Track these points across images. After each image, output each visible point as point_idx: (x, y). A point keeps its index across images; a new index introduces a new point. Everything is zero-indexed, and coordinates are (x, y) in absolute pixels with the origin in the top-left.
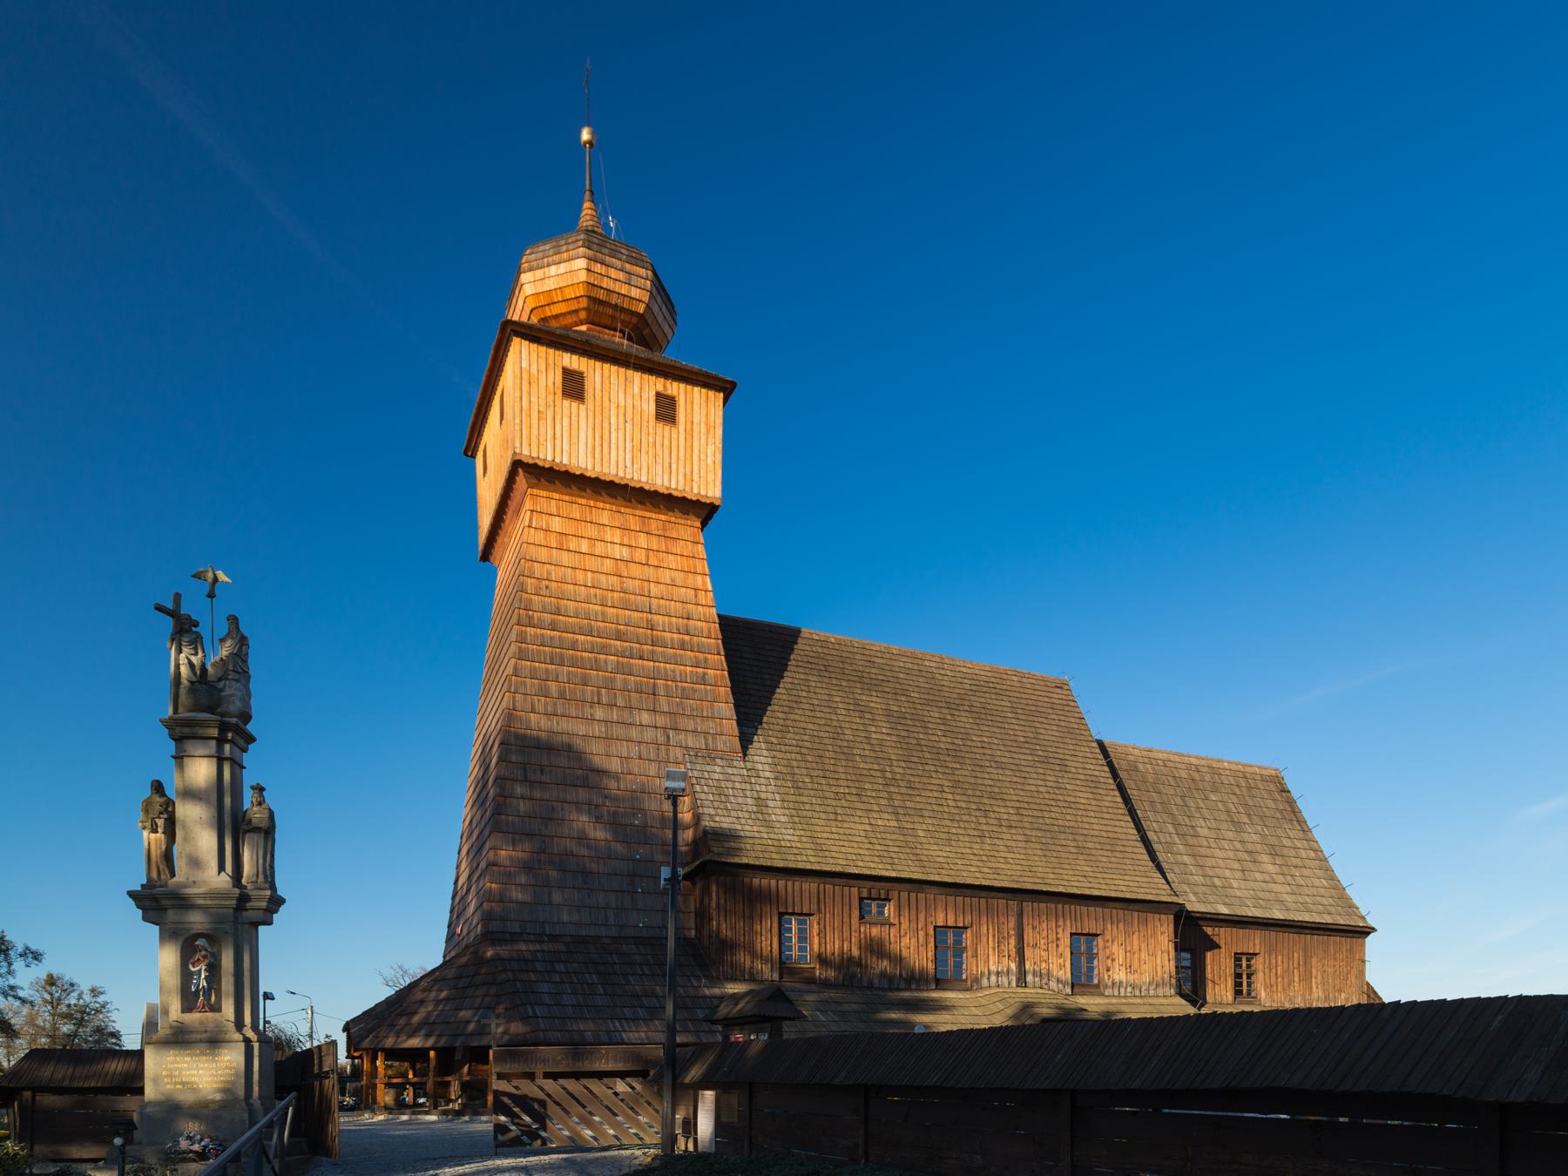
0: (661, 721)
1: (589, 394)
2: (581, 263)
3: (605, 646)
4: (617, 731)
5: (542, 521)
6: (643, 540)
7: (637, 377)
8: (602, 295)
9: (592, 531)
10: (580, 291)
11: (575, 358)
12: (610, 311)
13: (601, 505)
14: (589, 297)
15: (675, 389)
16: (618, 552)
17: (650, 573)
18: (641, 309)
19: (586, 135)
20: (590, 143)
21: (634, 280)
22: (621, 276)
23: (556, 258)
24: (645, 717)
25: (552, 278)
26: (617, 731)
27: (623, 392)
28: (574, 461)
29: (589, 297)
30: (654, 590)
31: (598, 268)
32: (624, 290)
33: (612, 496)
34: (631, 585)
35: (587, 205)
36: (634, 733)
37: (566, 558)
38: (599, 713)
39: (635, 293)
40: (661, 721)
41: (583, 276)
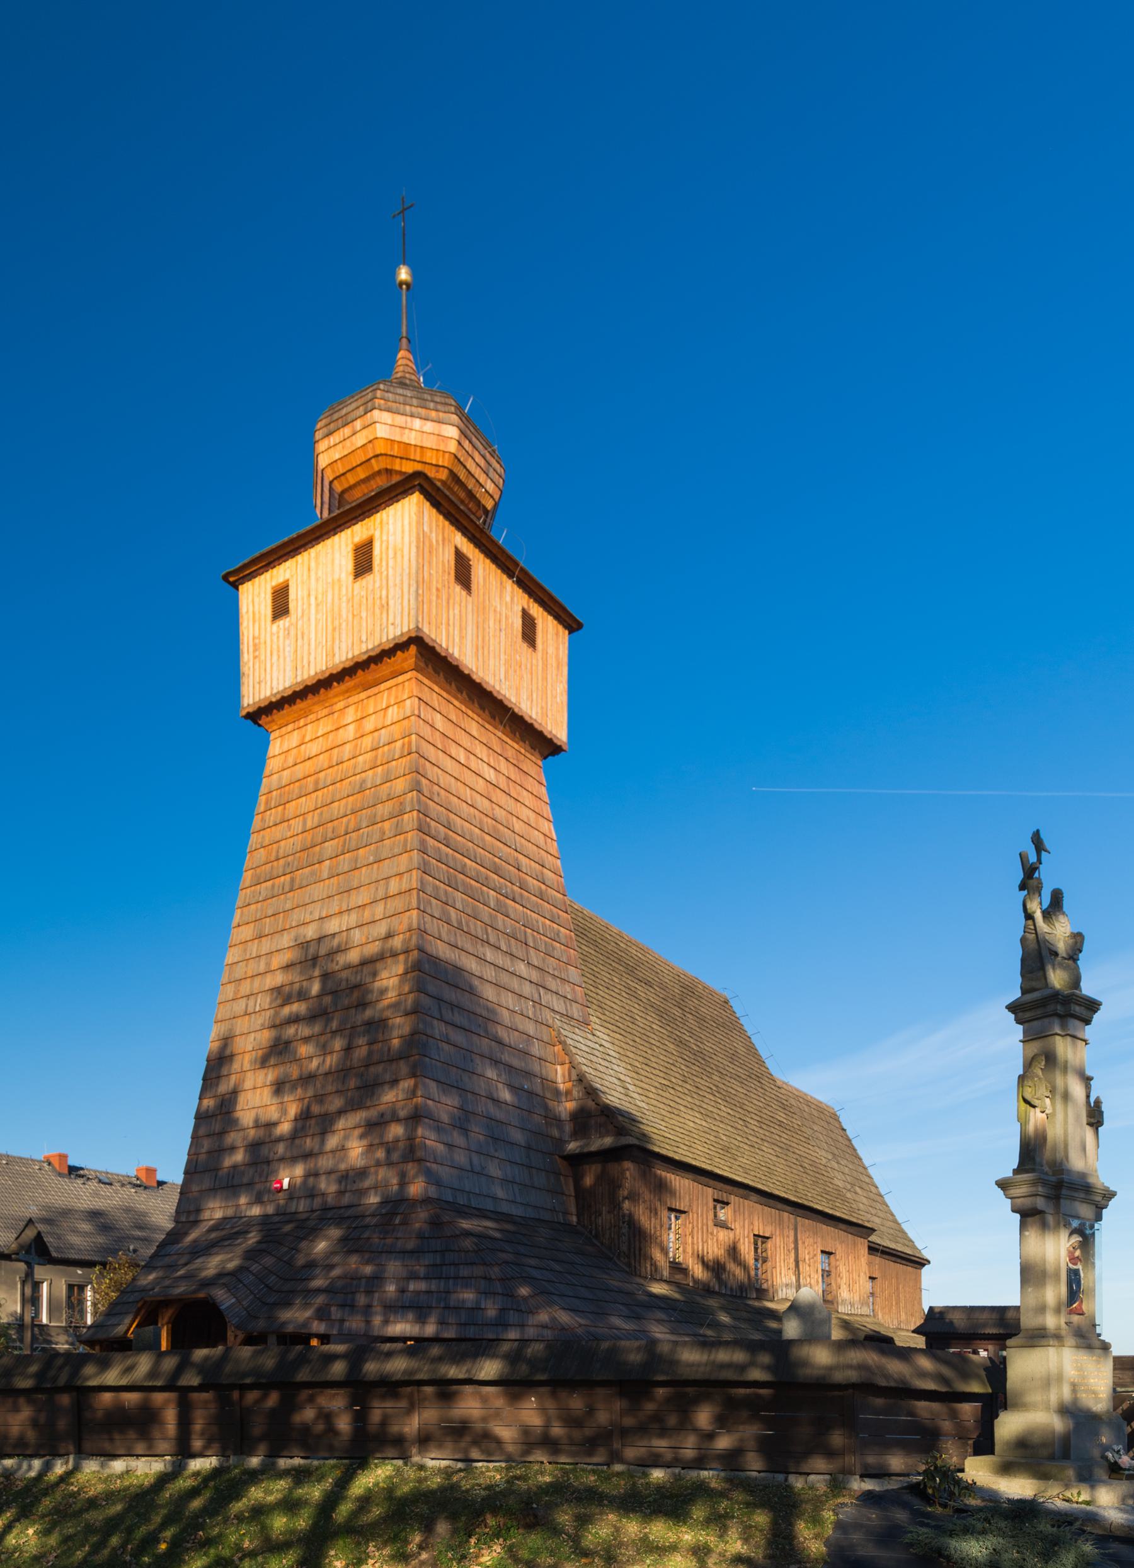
0: (534, 975)
1: (474, 586)
2: (452, 432)
3: (478, 873)
4: (505, 978)
5: (427, 714)
6: (503, 766)
7: (509, 585)
8: (462, 475)
9: (465, 741)
10: (445, 461)
11: (465, 540)
12: (462, 495)
13: (470, 713)
14: (451, 472)
15: (536, 610)
16: (490, 774)
17: (511, 804)
18: (489, 504)
19: (404, 274)
20: (408, 285)
21: (491, 473)
22: (482, 463)
23: (422, 411)
24: (522, 968)
25: (427, 433)
26: (505, 978)
27: (502, 598)
28: (462, 658)
29: (451, 472)
30: (518, 826)
31: (466, 444)
32: (482, 478)
33: (482, 708)
34: (499, 813)
35: (401, 354)
36: (515, 984)
37: (449, 764)
38: (490, 955)
39: (490, 486)
40: (534, 975)
41: (452, 447)
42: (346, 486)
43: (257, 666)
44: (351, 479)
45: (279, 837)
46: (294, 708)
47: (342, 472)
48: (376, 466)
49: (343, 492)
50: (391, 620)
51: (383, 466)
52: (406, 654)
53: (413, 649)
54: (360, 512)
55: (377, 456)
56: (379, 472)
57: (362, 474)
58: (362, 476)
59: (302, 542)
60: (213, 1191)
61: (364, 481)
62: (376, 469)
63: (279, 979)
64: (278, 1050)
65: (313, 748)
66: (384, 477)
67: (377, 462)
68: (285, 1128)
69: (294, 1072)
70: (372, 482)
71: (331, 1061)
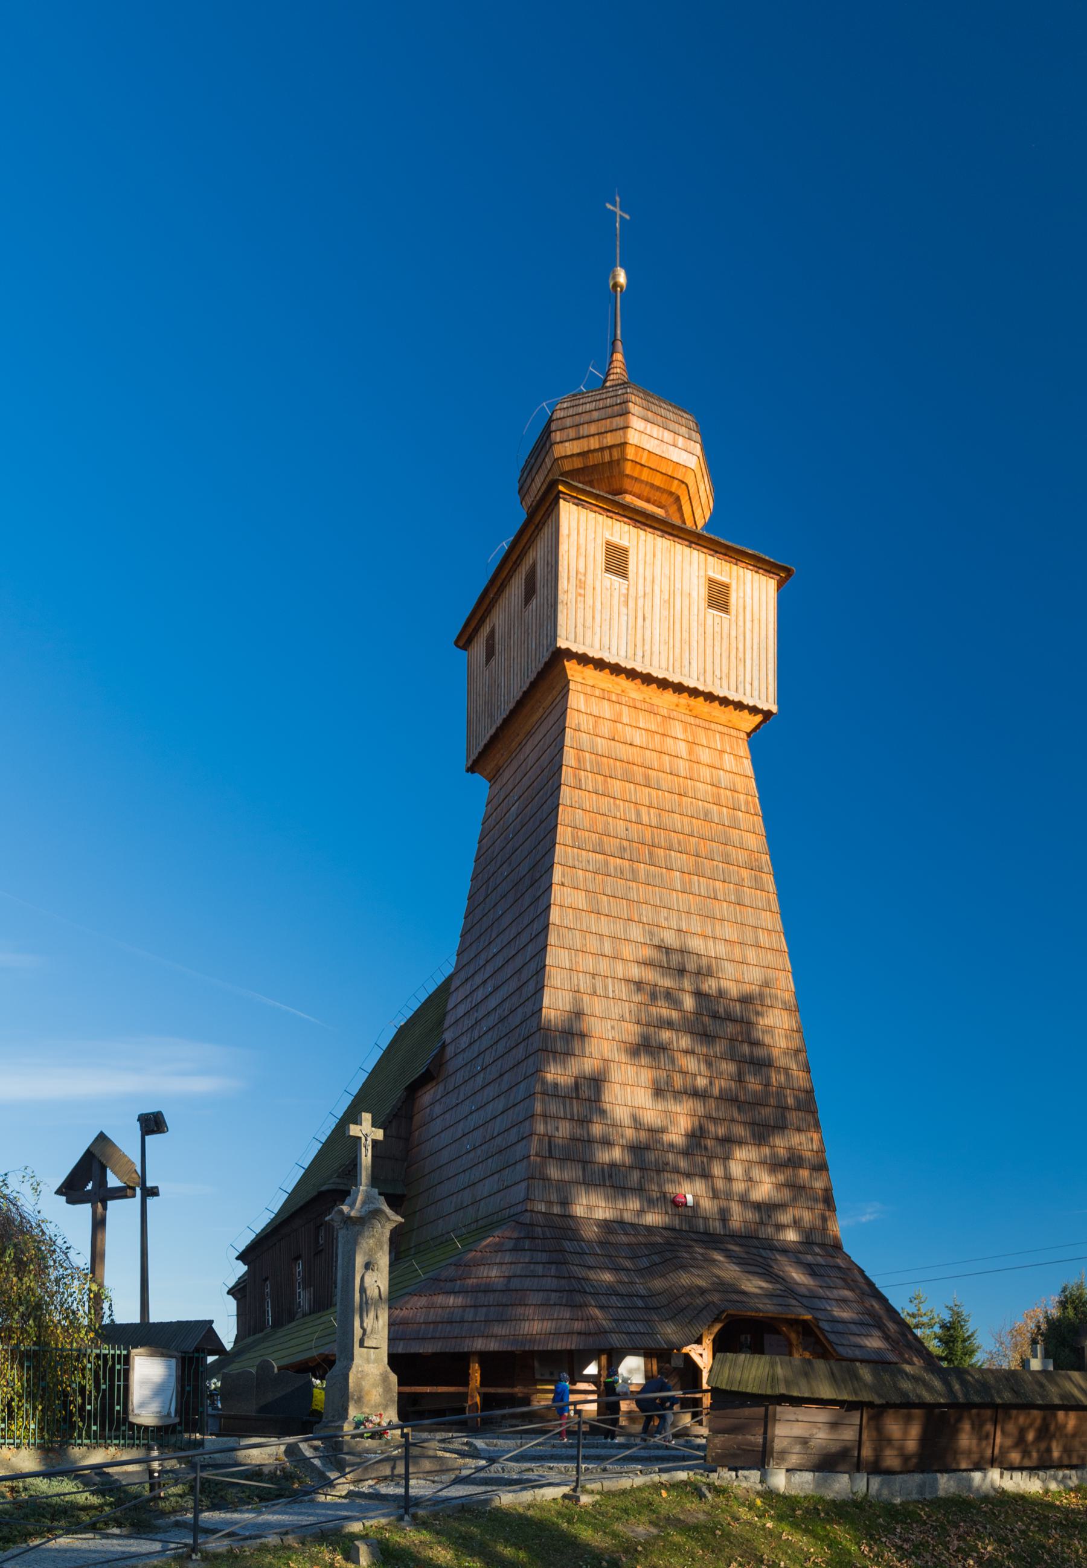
42: (636, 475)
43: (580, 605)
44: (645, 475)
45: (604, 809)
46: (613, 677)
47: (643, 462)
48: (674, 487)
49: (627, 476)
50: (748, 679)
51: (679, 493)
52: (750, 717)
53: (759, 718)
54: (723, 551)
55: (683, 482)
56: (671, 493)
57: (658, 481)
58: (657, 483)
59: (656, 525)
60: (589, 1183)
61: (652, 486)
62: (673, 490)
63: (635, 972)
64: (645, 1048)
65: (638, 738)
66: (672, 500)
67: (679, 486)
68: (676, 1136)
69: (678, 1081)
70: (658, 494)
71: (719, 1084)
